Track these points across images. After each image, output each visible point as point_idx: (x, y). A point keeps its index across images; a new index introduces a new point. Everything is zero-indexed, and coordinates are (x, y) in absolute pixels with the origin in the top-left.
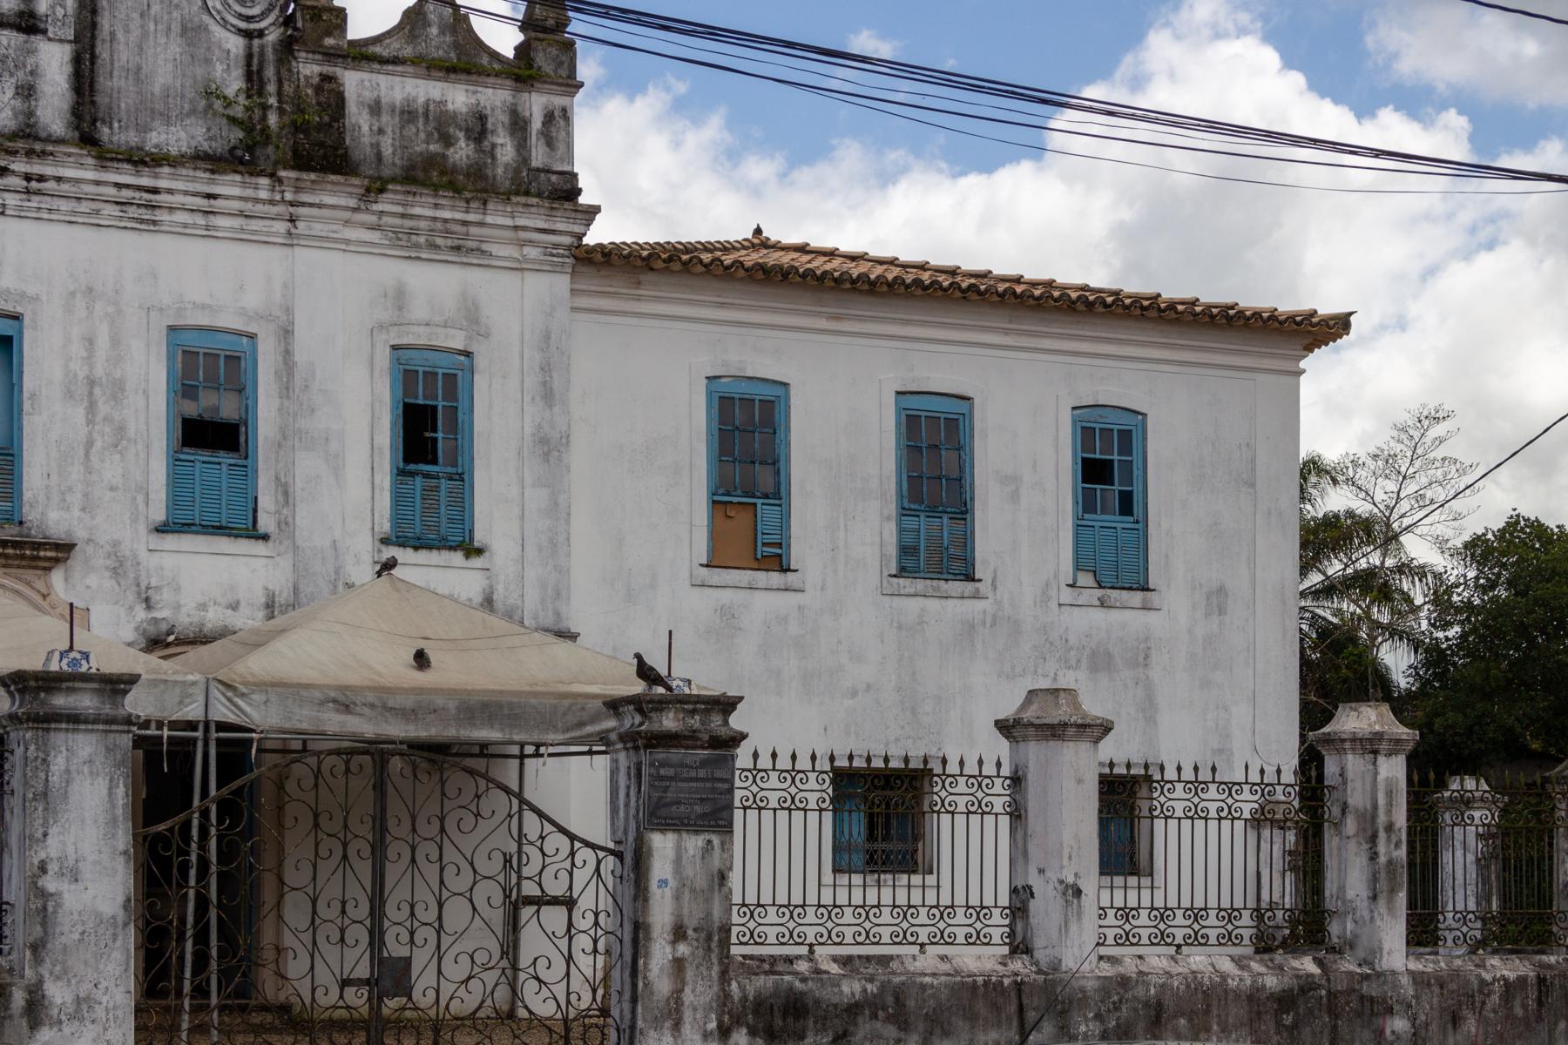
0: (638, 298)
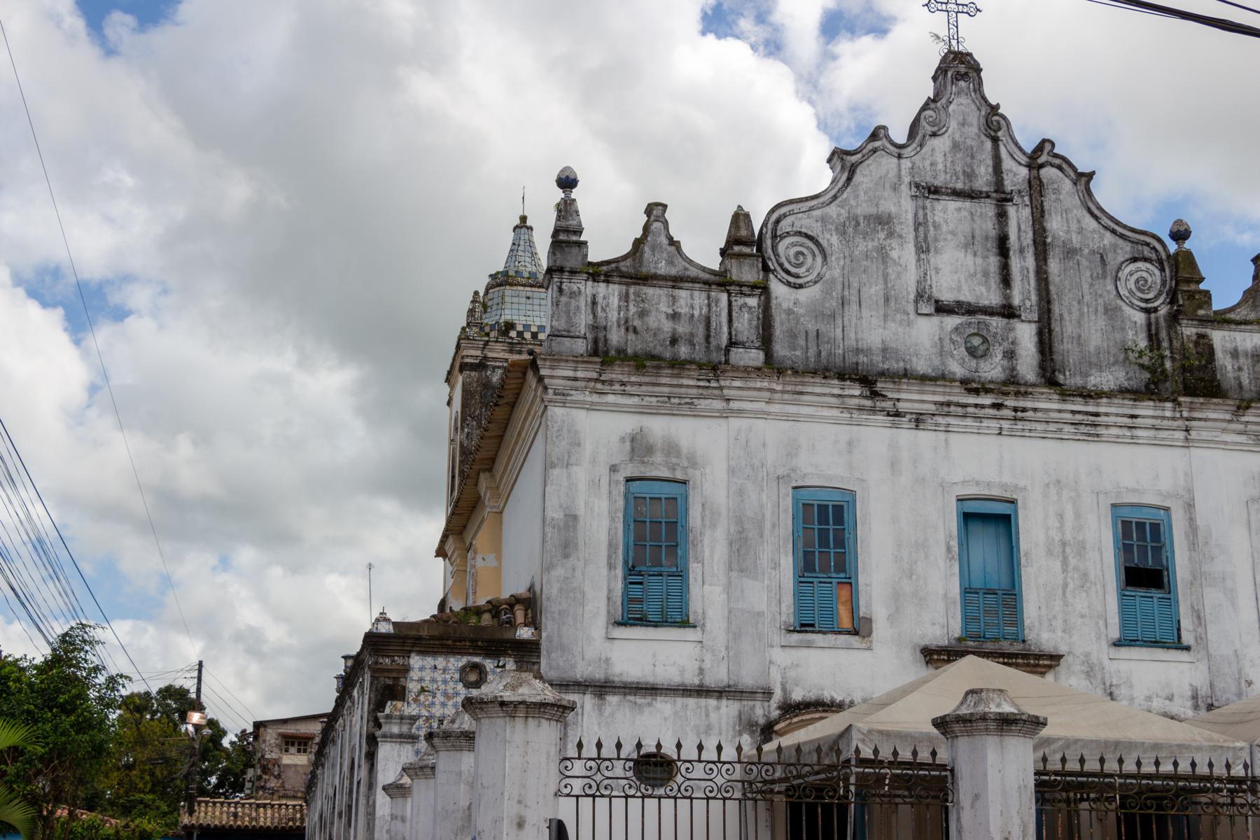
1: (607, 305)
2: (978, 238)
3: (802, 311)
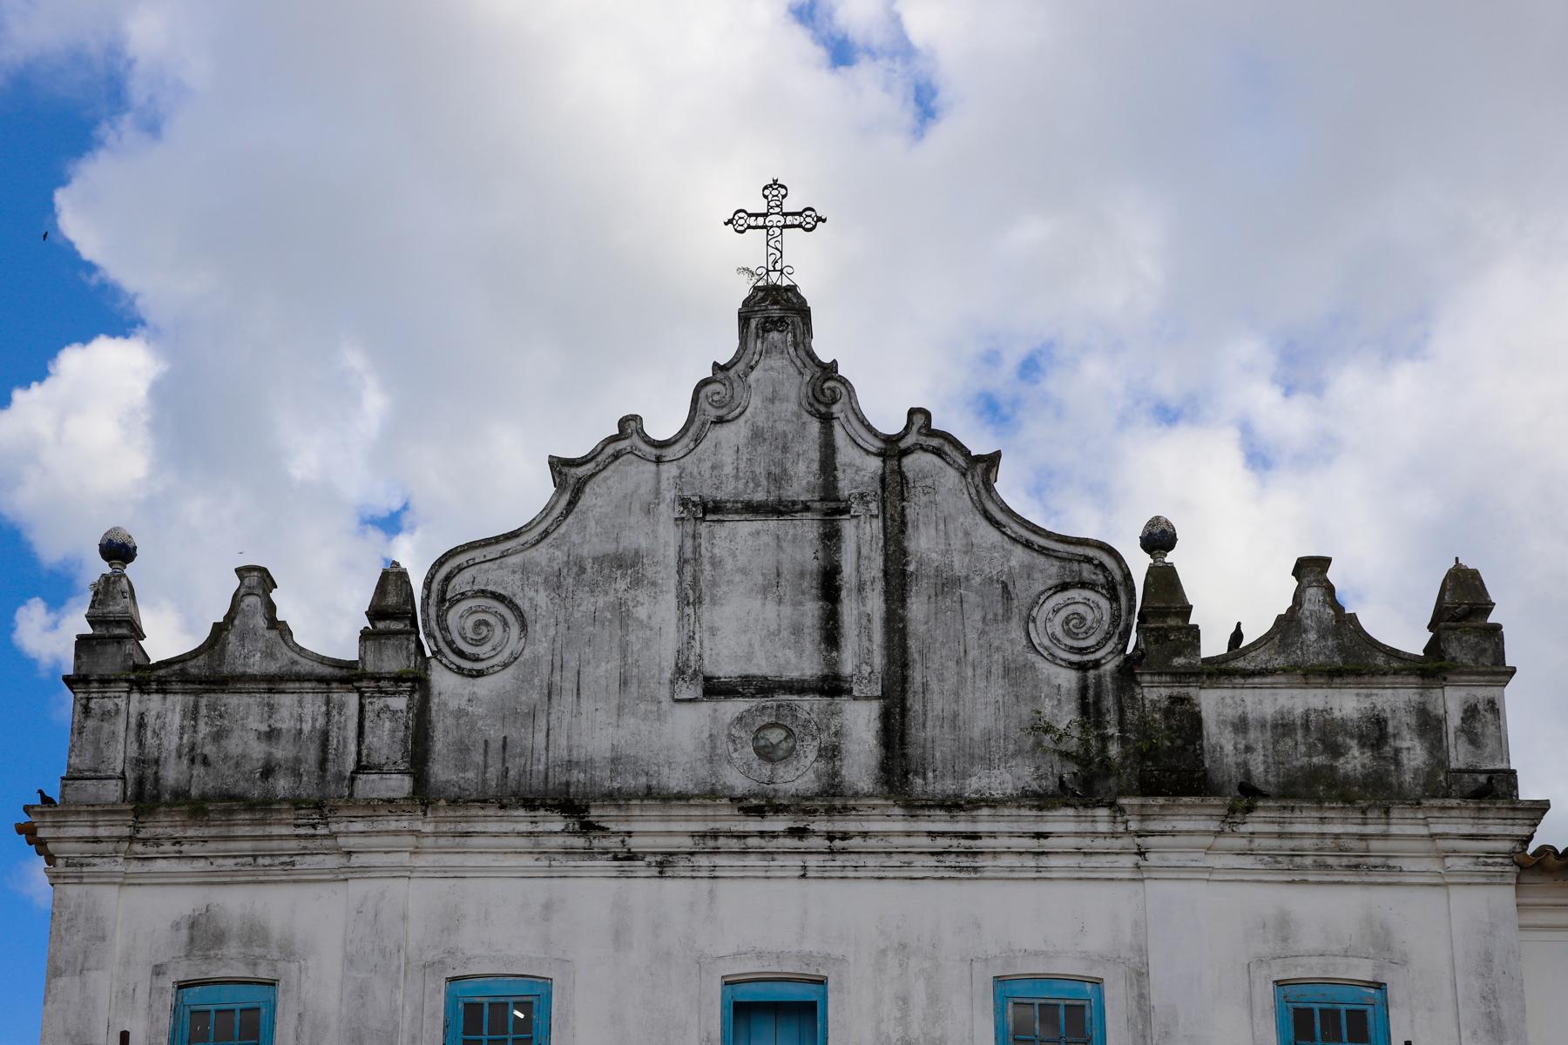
1: (163, 727)
3: (481, 711)
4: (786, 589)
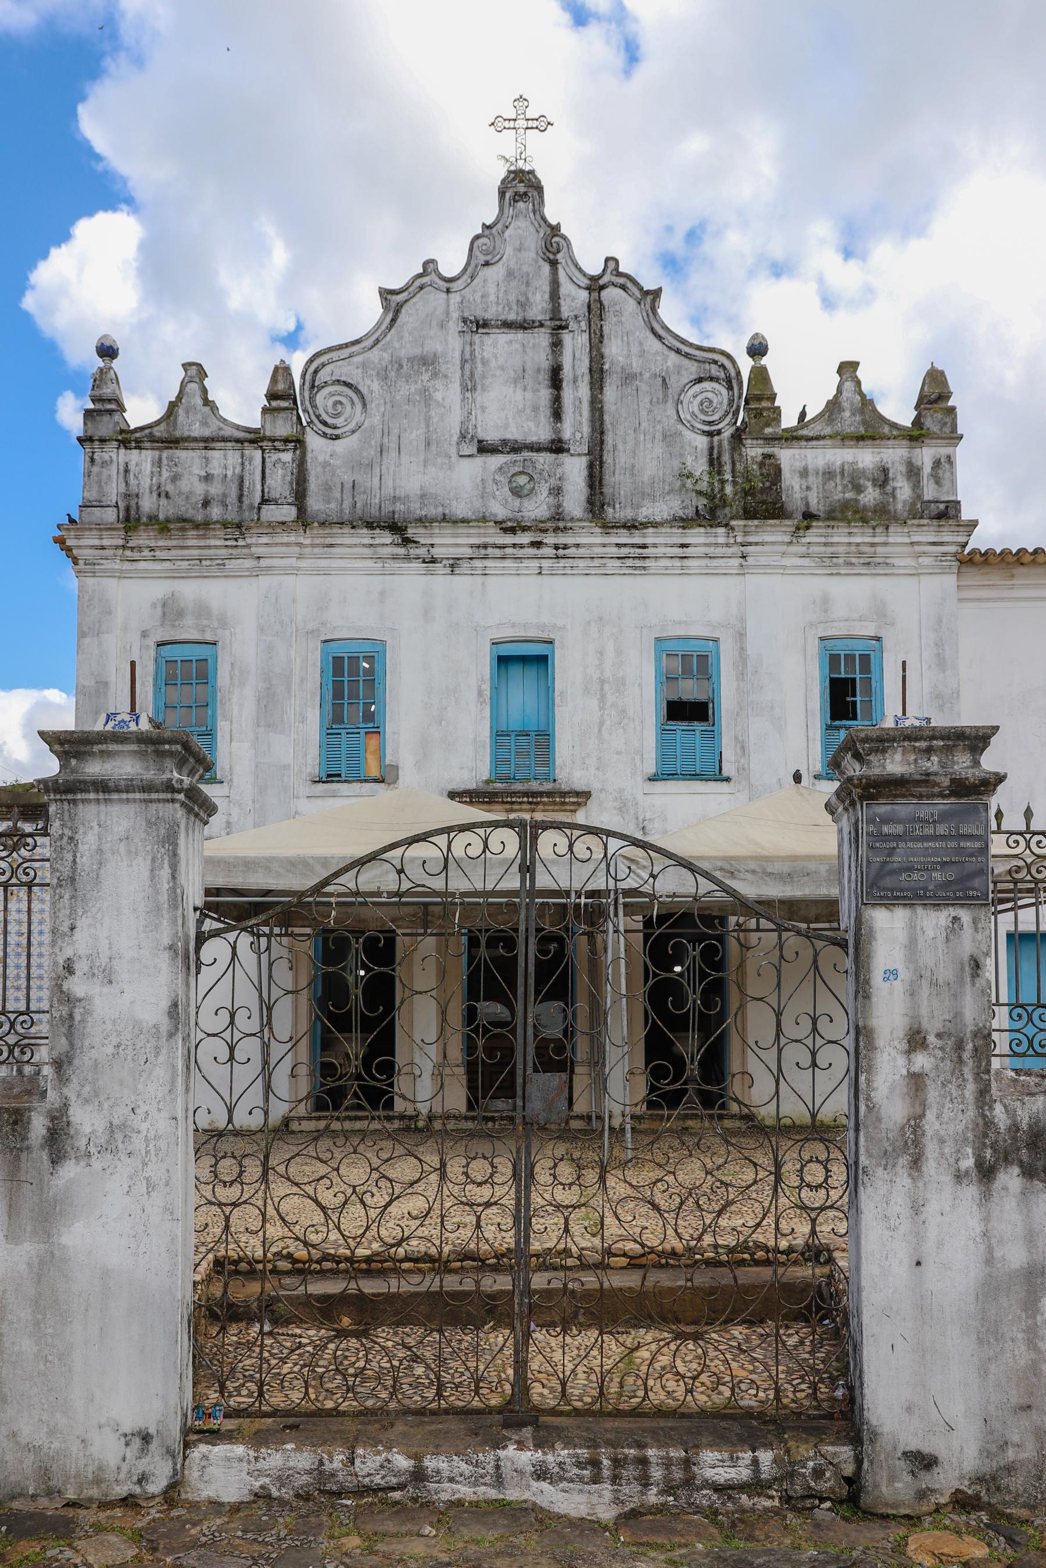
0: (1012, 587)
2: (529, 371)
4: (529, 380)
